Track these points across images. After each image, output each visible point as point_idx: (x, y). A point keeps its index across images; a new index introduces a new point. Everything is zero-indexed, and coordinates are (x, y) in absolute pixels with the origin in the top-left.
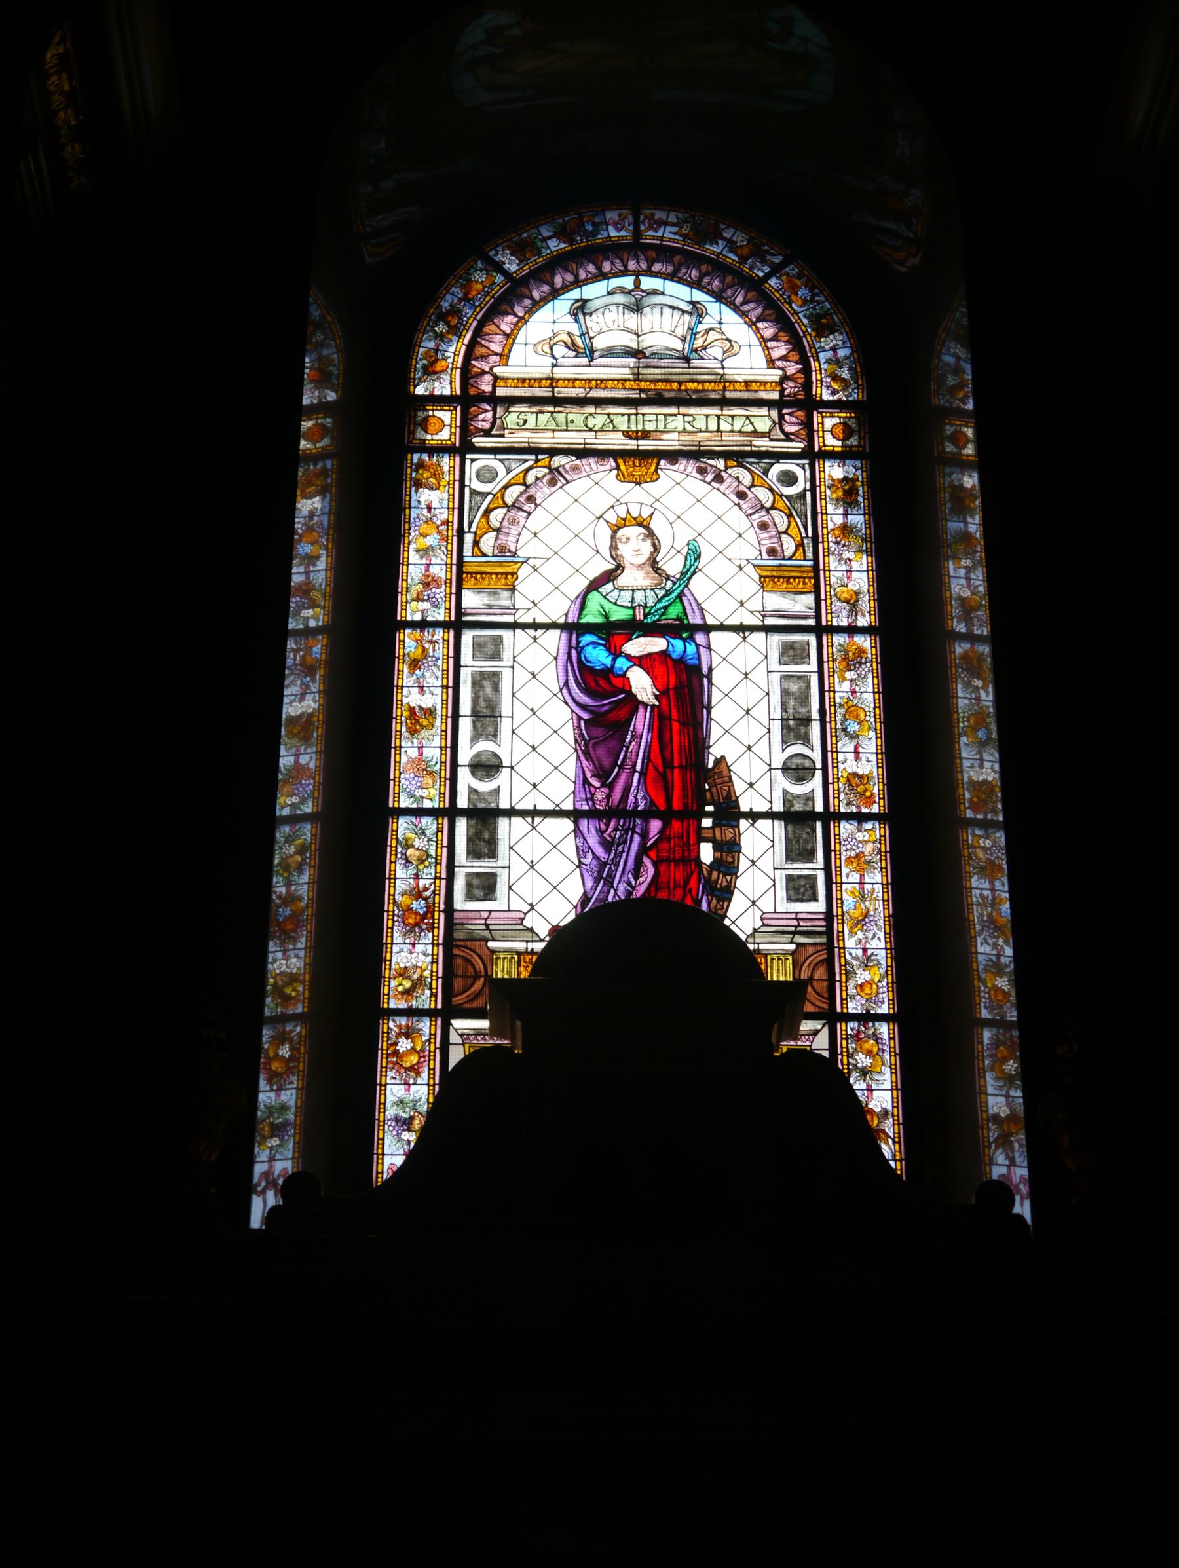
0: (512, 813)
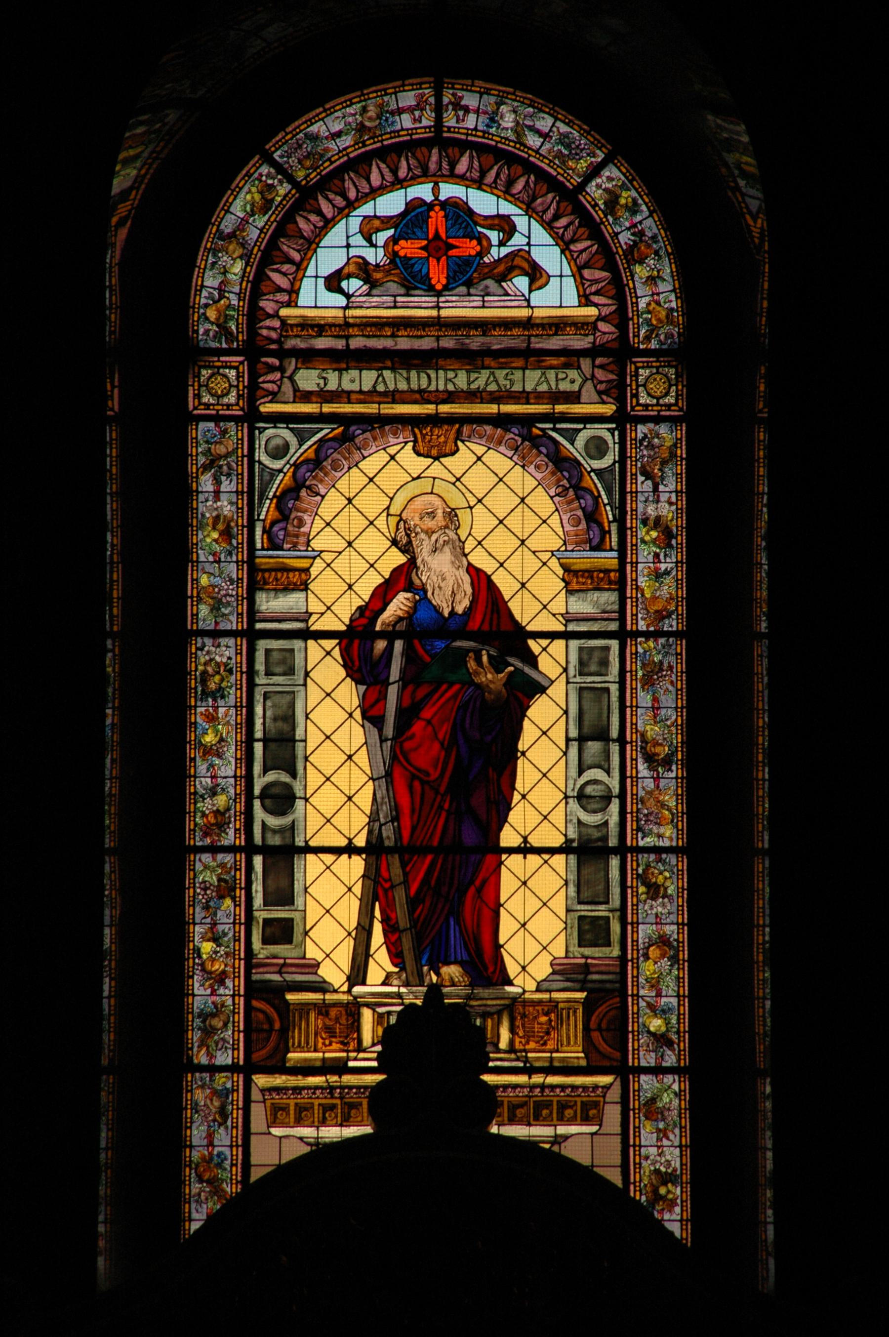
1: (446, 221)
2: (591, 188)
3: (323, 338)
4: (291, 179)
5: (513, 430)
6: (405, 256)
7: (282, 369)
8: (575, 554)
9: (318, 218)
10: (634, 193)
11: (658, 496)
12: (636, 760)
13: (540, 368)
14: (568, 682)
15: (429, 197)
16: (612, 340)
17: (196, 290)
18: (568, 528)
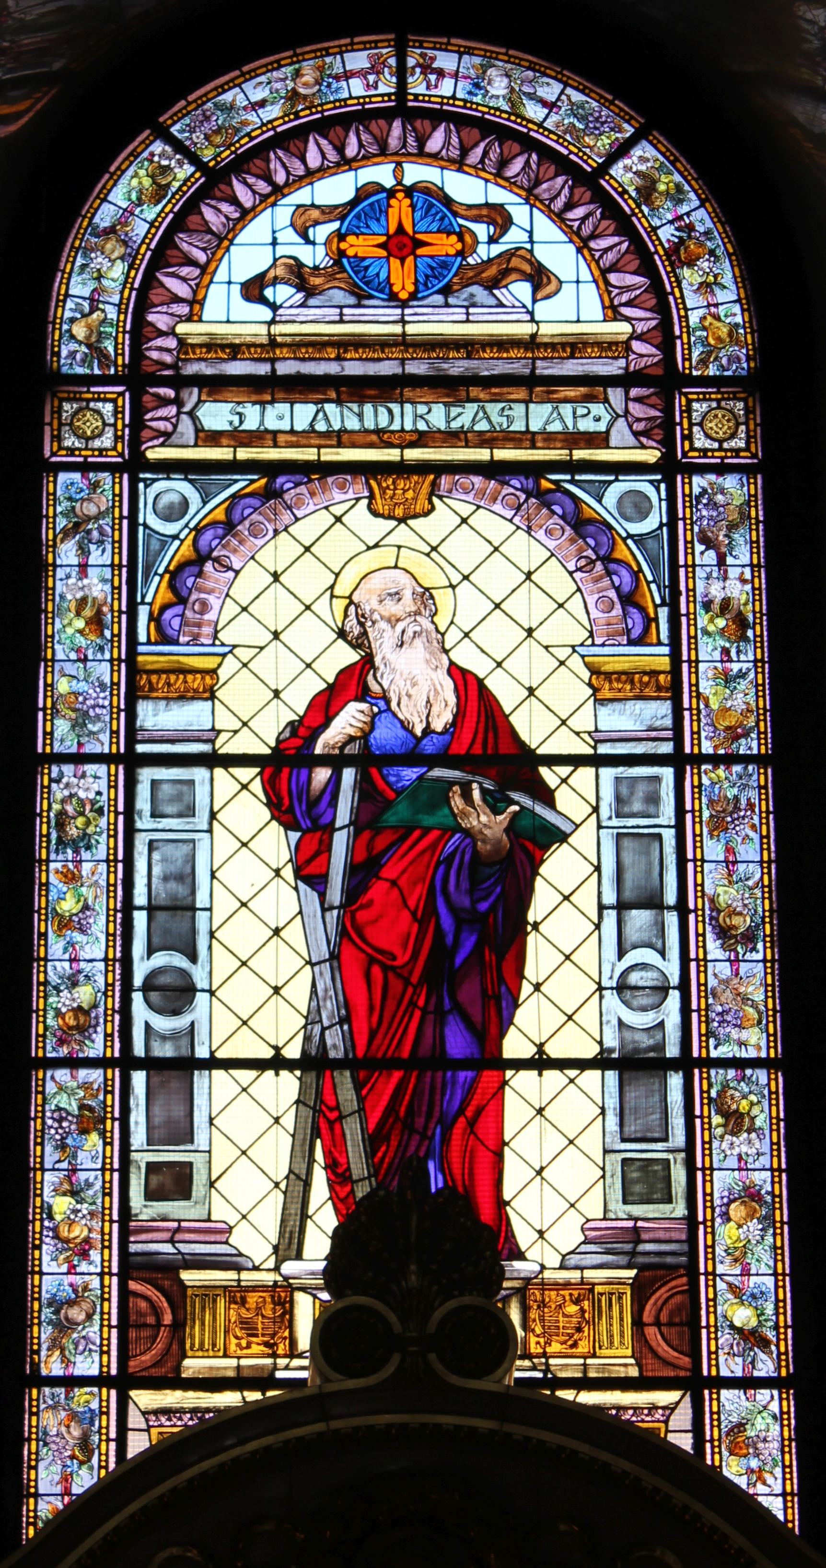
0: (213, 1063)
1: (413, 212)
2: (617, 170)
3: (238, 363)
4: (194, 159)
5: (513, 482)
6: (356, 256)
7: (178, 402)
8: (606, 650)
9: (232, 208)
10: (677, 178)
11: (726, 572)
12: (704, 935)
13: (549, 401)
14: (600, 827)
15: (389, 182)
16: (652, 365)
17: (58, 301)
18: (595, 613)
